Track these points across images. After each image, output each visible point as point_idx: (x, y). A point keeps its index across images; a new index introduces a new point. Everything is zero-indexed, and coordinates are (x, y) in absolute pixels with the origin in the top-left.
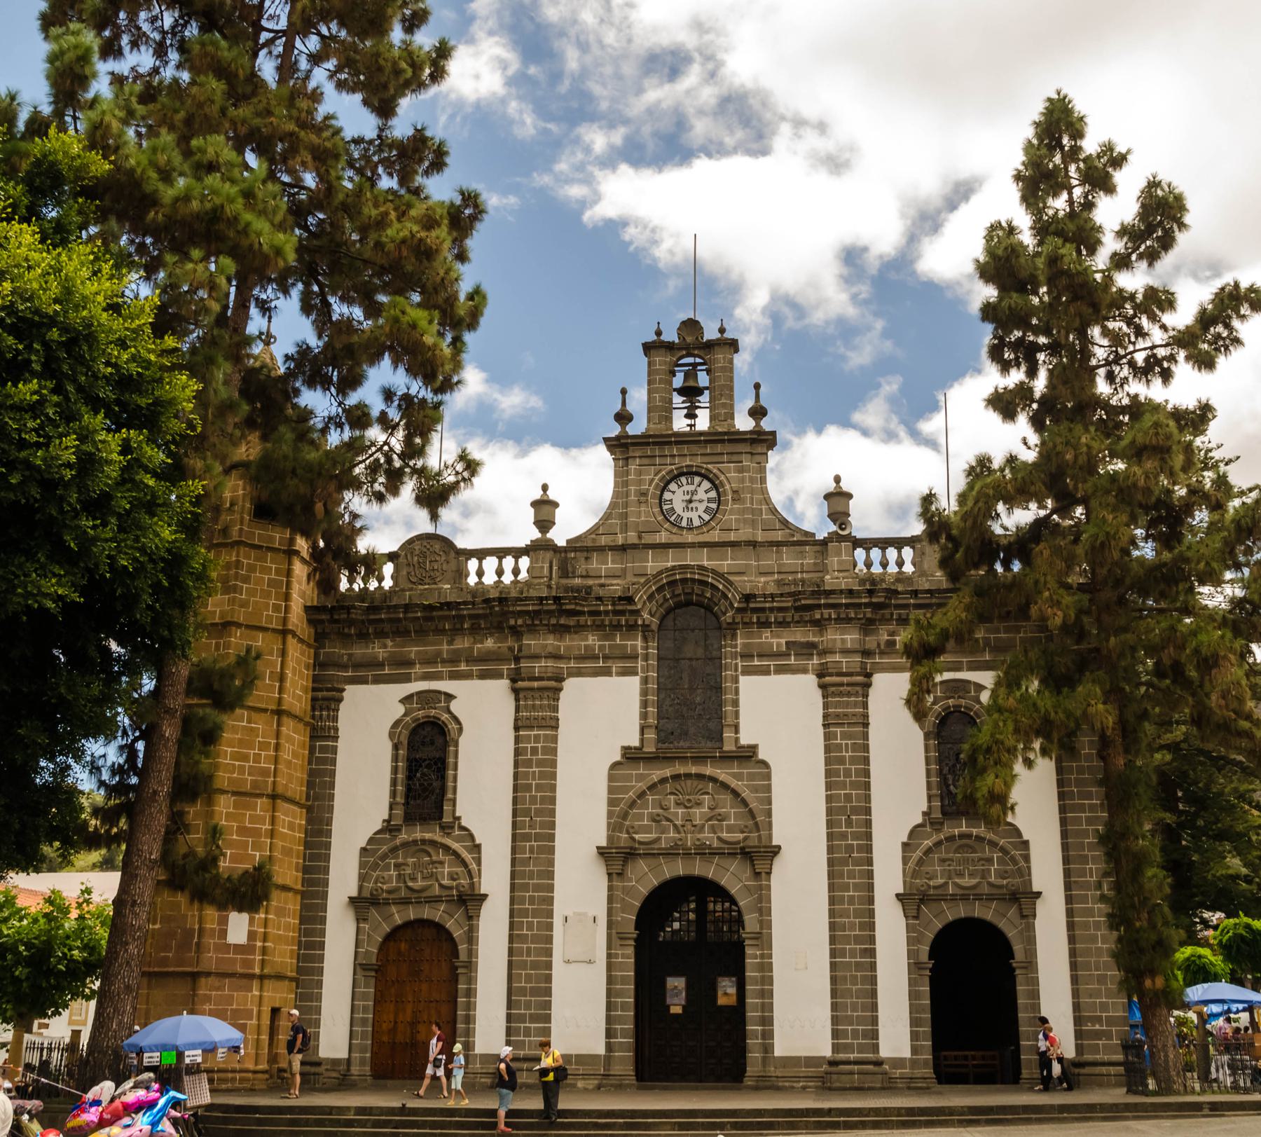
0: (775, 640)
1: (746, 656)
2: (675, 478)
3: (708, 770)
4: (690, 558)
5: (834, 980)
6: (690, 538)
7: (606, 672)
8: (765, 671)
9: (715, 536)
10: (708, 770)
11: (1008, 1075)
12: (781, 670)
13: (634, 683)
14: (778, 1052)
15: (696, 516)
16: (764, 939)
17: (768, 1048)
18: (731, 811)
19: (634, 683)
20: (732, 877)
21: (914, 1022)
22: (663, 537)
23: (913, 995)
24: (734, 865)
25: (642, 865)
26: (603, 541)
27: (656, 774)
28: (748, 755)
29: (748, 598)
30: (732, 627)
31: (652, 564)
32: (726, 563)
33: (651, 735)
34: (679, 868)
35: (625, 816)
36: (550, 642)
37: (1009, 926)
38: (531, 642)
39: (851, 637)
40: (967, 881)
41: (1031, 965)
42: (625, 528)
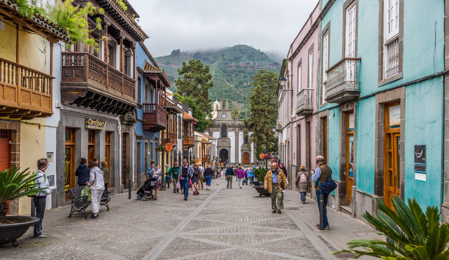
0: (231, 129)
1: (229, 130)
2: (223, 114)
3: (226, 140)
4: (224, 122)
5: (235, 157)
6: (224, 120)
7: (217, 131)
8: (230, 132)
9: (226, 119)
10: (226, 140)
11: (249, 164)
12: (232, 132)
13: (219, 132)
14: (231, 162)
15: (225, 117)
16: (230, 154)
17: (230, 162)
18: (227, 143)
19: (219, 132)
20: (227, 149)
21: (241, 160)
22: (222, 119)
23: (241, 158)
24: (228, 148)
25: (220, 148)
26: (216, 119)
27: (221, 140)
28: (229, 139)
29: (229, 126)
30: (228, 128)
31: (221, 122)
32: (227, 122)
33: (221, 137)
34: (223, 148)
35: (218, 144)
36: (212, 129)
37: (249, 152)
38: (210, 129)
39: (237, 129)
40: (246, 149)
41: (251, 156)
42: (218, 118)
